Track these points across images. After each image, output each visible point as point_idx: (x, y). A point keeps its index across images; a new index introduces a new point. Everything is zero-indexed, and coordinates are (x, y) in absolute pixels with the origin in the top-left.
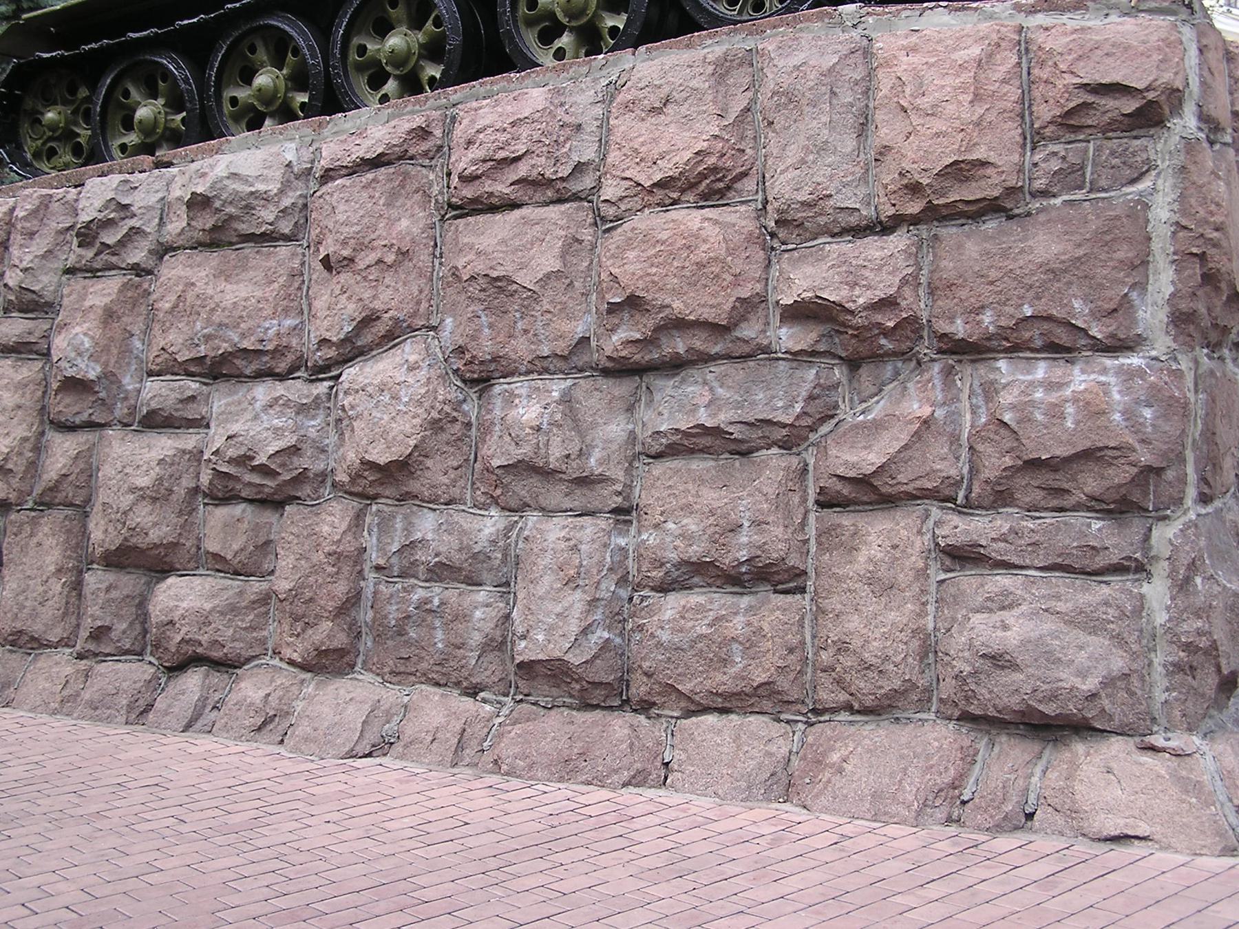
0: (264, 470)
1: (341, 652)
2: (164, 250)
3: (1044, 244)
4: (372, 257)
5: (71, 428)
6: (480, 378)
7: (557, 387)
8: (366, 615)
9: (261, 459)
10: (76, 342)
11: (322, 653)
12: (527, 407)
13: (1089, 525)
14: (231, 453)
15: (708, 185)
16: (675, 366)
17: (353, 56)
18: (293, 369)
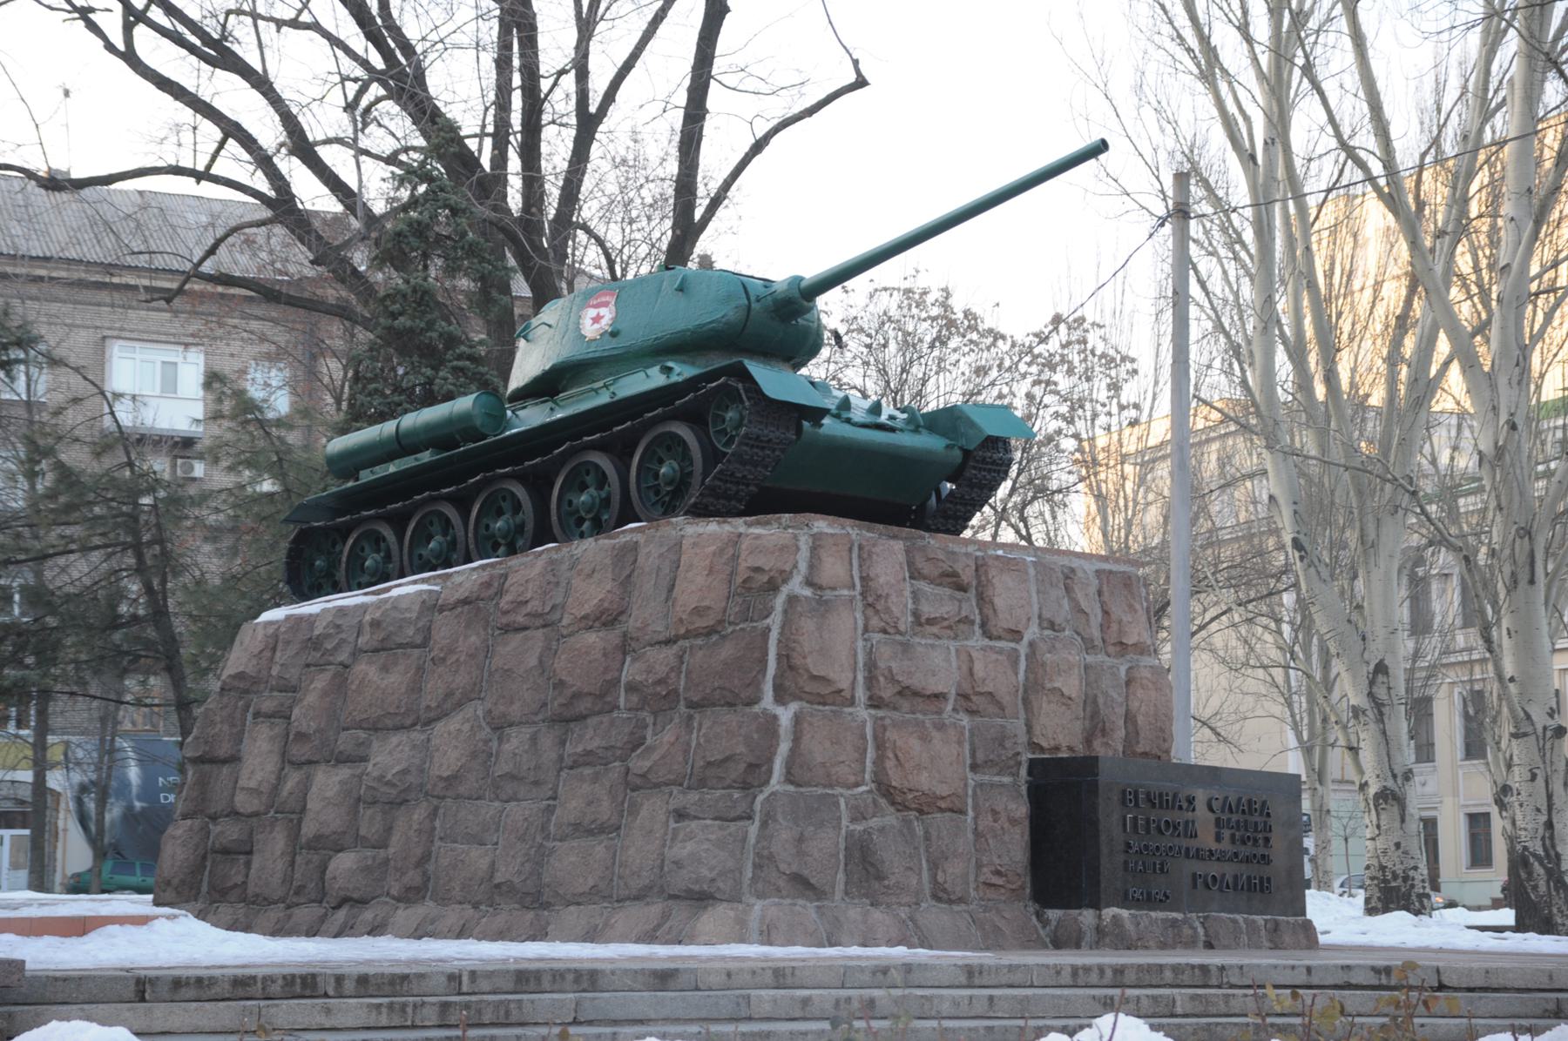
0: (388, 783)
1: (417, 890)
2: (356, 653)
3: (727, 651)
4: (454, 658)
5: (298, 765)
6: (500, 726)
7: (527, 732)
8: (431, 867)
9: (389, 777)
10: (307, 713)
11: (408, 889)
12: (517, 740)
13: (731, 795)
14: (375, 774)
15: (607, 619)
16: (581, 718)
17: (483, 531)
18: (414, 724)
